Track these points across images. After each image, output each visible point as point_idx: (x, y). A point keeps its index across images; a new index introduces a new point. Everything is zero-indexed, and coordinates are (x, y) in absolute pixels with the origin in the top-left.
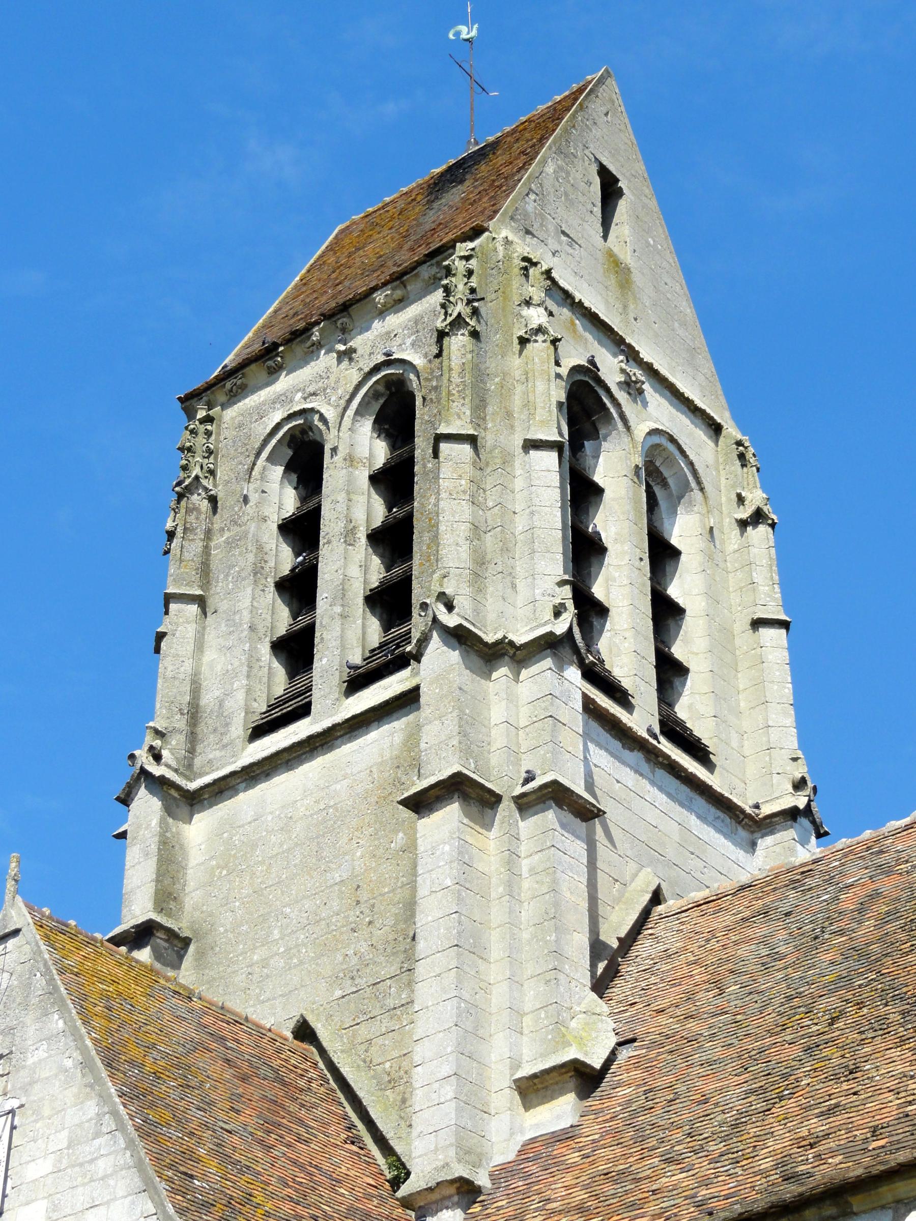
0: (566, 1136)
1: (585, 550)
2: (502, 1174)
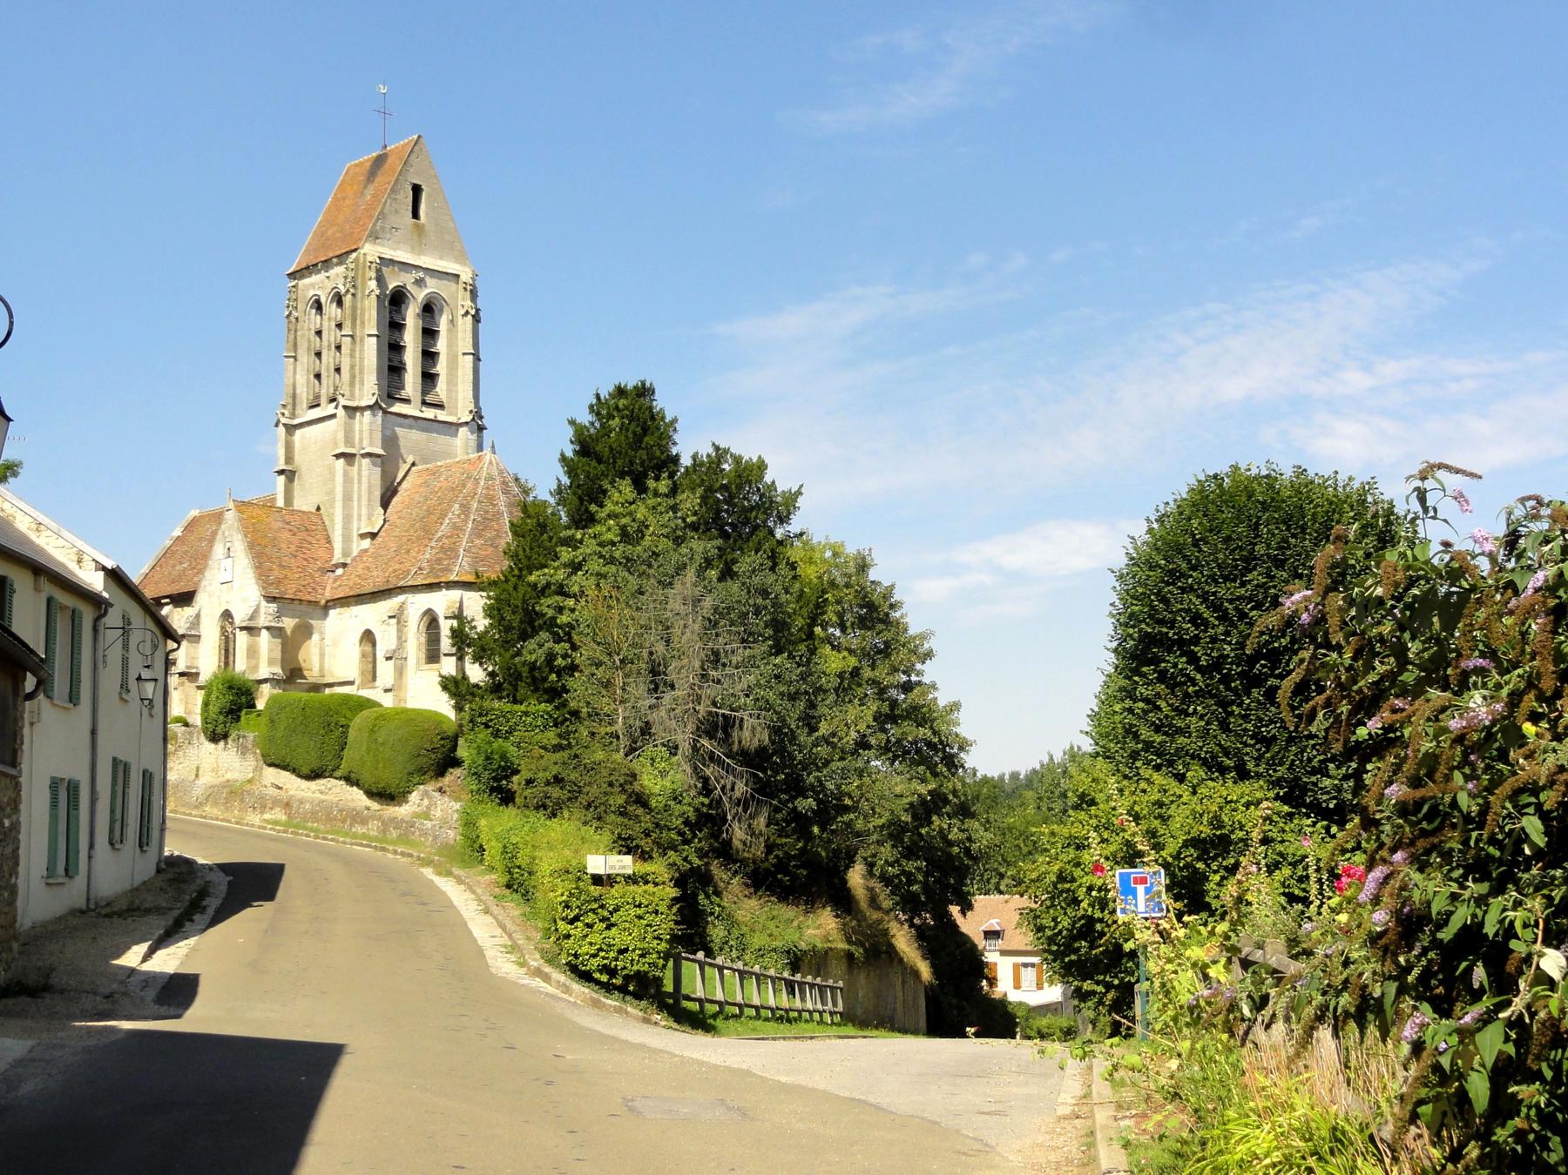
0: (366, 551)
1: (396, 348)
2: (354, 559)
